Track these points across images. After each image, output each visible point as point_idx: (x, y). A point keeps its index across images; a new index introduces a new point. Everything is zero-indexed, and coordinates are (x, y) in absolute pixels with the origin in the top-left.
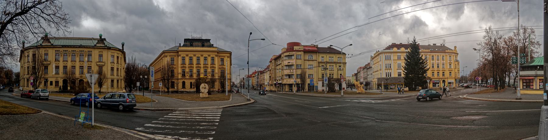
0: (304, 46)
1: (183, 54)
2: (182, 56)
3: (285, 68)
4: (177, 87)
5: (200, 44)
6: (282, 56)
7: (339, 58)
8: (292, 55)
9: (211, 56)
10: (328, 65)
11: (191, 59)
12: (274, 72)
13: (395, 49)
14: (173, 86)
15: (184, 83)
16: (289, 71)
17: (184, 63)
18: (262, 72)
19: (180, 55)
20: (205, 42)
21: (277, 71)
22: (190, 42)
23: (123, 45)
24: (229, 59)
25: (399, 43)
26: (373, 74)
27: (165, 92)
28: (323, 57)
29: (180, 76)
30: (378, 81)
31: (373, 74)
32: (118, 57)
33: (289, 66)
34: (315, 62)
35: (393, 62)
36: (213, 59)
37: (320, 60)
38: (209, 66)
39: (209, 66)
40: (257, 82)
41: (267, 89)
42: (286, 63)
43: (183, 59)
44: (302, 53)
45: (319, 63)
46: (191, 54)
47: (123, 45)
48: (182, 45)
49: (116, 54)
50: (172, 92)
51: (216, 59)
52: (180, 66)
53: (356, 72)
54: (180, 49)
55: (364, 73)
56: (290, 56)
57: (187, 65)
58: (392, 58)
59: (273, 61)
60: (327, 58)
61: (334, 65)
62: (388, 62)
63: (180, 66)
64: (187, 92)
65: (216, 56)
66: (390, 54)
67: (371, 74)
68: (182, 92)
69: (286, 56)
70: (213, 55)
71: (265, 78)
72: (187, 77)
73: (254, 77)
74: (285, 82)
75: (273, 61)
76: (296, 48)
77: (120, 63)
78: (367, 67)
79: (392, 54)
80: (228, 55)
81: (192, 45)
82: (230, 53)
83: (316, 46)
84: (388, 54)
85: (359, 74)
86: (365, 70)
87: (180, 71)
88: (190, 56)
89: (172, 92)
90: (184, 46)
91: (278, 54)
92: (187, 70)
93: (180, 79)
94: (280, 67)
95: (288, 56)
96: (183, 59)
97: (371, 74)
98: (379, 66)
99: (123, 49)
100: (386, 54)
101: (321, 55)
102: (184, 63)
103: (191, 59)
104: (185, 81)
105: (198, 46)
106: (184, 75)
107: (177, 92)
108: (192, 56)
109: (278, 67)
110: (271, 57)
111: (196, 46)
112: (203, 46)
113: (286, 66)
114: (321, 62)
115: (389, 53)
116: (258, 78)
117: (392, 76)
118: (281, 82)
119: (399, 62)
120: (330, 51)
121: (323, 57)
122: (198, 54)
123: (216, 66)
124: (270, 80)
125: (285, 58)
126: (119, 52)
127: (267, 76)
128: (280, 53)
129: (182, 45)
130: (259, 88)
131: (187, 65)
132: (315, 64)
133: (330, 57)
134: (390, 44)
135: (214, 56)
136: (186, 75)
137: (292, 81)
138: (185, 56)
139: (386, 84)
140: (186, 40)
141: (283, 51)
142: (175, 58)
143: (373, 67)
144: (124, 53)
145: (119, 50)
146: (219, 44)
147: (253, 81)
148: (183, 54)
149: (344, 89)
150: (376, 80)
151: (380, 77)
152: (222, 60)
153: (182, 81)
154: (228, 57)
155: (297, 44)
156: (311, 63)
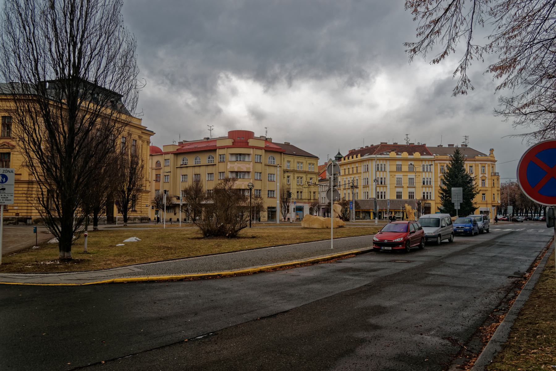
7: (310, 164)
35: (388, 174)
58: (388, 169)
66: (384, 162)
79: (388, 163)
84: (381, 162)
100: (378, 162)
119: (399, 175)
121: (289, 162)
133: (298, 163)
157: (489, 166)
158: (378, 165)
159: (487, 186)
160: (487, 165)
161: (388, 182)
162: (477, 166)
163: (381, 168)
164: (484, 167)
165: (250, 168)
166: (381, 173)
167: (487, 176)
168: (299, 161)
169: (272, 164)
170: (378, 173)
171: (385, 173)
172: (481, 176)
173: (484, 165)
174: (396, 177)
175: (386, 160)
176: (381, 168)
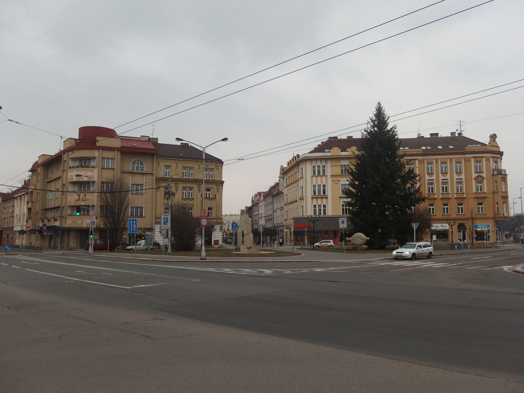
0: (124, 139)
3: (70, 188)
6: (65, 157)
8: (90, 159)
10: (180, 186)
13: (336, 151)
21: (50, 196)
25: (345, 137)
26: (286, 208)
28: (167, 167)
30: (296, 226)
31: (286, 208)
33: (83, 185)
34: (149, 177)
35: (330, 179)
37: (161, 175)
42: (72, 175)
44: (117, 155)
45: (159, 180)
53: (250, 204)
55: (266, 206)
58: (329, 171)
60: (177, 169)
61: (195, 186)
62: (319, 181)
67: (282, 209)
69: (74, 159)
74: (69, 223)
76: (102, 141)
78: (274, 193)
83: (154, 141)
84: (319, 163)
85: (255, 209)
86: (269, 200)
94: (58, 185)
95: (81, 159)
97: (282, 209)
98: (300, 190)
100: (314, 164)
101: (163, 163)
109: (53, 186)
113: (74, 183)
114: (164, 180)
115: (321, 159)
117: (330, 213)
118: (57, 224)
120: (186, 153)
124: (29, 218)
125: (71, 164)
127: (20, 209)
132: (146, 181)
133: (185, 168)
134: (325, 139)
139: (310, 231)
141: (68, 146)
143: (285, 191)
149: (216, 242)
150: (292, 222)
151: (300, 215)
155: (109, 133)
156: (138, 179)
157: (488, 160)
158: (314, 167)
159: (486, 191)
160: (484, 159)
161: (329, 193)
162: (468, 160)
163: (319, 171)
164: (480, 161)
165: (93, 176)
166: (319, 178)
167: (484, 175)
168: (185, 165)
169: (140, 171)
170: (314, 178)
171: (324, 178)
172: (474, 175)
173: (478, 159)
174: (342, 183)
175: (326, 159)
176: (319, 171)
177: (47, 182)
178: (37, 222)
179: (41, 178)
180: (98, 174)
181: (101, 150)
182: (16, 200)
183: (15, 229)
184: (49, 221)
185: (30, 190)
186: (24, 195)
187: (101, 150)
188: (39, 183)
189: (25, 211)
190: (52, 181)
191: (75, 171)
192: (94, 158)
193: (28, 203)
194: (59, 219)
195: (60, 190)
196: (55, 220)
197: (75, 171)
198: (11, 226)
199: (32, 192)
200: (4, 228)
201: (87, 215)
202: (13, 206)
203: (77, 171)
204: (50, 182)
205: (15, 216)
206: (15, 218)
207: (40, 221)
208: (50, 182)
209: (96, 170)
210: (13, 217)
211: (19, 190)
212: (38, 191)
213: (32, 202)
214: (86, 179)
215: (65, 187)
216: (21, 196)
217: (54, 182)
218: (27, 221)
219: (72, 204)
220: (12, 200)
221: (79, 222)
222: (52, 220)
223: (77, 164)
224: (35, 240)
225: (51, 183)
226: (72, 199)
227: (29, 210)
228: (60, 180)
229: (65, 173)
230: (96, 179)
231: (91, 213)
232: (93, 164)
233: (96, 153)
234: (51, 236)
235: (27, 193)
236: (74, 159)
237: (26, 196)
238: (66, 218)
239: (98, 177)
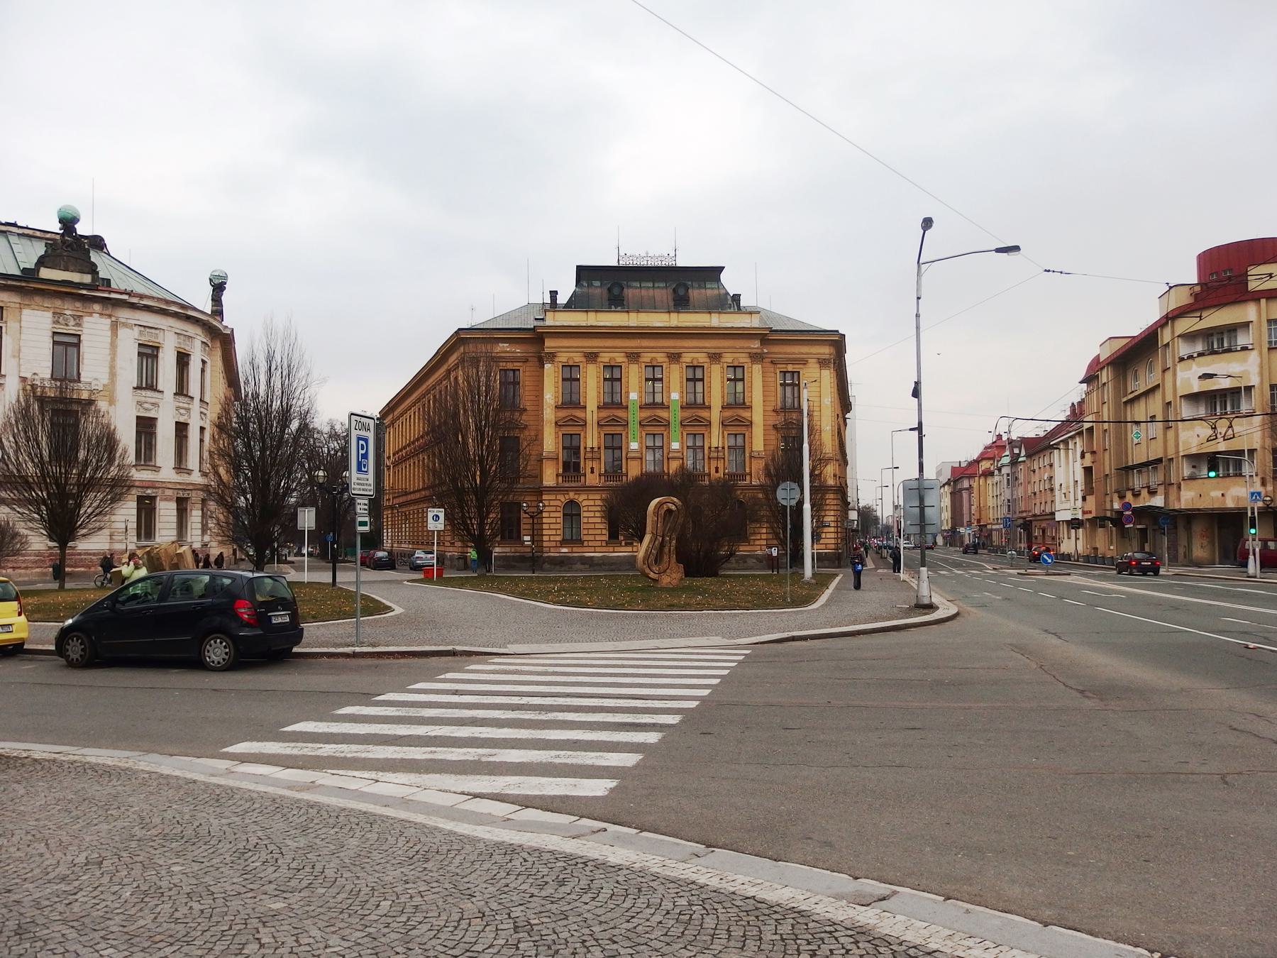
1: (568, 351)
2: (563, 358)
3: (1186, 411)
4: (537, 534)
5: (662, 293)
6: (1166, 336)
8: (1232, 329)
9: (728, 358)
11: (613, 377)
12: (1110, 442)
14: (510, 531)
15: (572, 513)
16: (1204, 430)
17: (571, 402)
18: (1037, 447)
19: (552, 357)
20: (688, 284)
21: (1134, 434)
22: (605, 284)
23: (218, 288)
24: (828, 376)
27: (464, 563)
29: (550, 476)
32: (183, 360)
33: (1219, 401)
36: (737, 375)
38: (715, 415)
39: (715, 415)
40: (1011, 504)
41: (1067, 546)
43: (571, 378)
46: (613, 353)
47: (218, 288)
48: (562, 299)
49: (169, 339)
50: (508, 563)
51: (756, 373)
52: (549, 414)
54: (553, 320)
56: (1219, 341)
57: (591, 411)
59: (1105, 376)
63: (549, 414)
64: (590, 563)
65: (756, 357)
68: (562, 562)
69: (1190, 337)
70: (735, 353)
71: (1060, 476)
72: (592, 480)
73: (988, 474)
74: (1187, 498)
75: (1105, 376)
77: (194, 388)
80: (826, 351)
81: (616, 302)
82: (837, 343)
87: (550, 442)
88: (605, 358)
89: (508, 563)
90: (572, 305)
91: (1135, 327)
92: (592, 439)
93: (551, 490)
94: (1154, 406)
96: (571, 378)
99: (218, 312)
102: (571, 402)
103: (613, 377)
104: (581, 498)
105: (653, 307)
106: (571, 468)
107: (534, 561)
108: (620, 358)
109: (1140, 412)
110: (1091, 345)
111: (640, 307)
112: (681, 303)
113: (1194, 398)
116: (1013, 480)
118: (1158, 501)
122: (654, 352)
123: (758, 416)
124: (1089, 490)
125: (1184, 349)
126: (192, 330)
127: (1067, 469)
128: (1152, 315)
129: (562, 299)
130: (1029, 537)
131: (591, 411)
135: (743, 359)
136: (586, 466)
137: (1235, 494)
138: (578, 358)
140: (584, 273)
142: (526, 376)
144: (224, 341)
145: (184, 314)
146: (768, 286)
147: (992, 499)
148: (568, 351)
152: (792, 382)
153: (563, 498)
154: (823, 363)
177: (1126, 403)
178: (1108, 499)
179: (1109, 393)
180: (1261, 367)
181: (1263, 301)
182: (1056, 452)
183: (1058, 517)
184: (1136, 495)
185: (1087, 426)
186: (1072, 437)
187: (1263, 301)
188: (1106, 406)
189: (1080, 475)
190: (1137, 398)
191: (1194, 367)
192: (1246, 325)
193: (1083, 456)
194: (1161, 489)
195: (1160, 417)
196: (1152, 493)
197: (1194, 367)
198: (1048, 510)
199: (1090, 430)
200: (1035, 515)
201: (1236, 475)
202: (1051, 465)
203: (1199, 365)
204: (1132, 401)
205: (1057, 487)
206: (1057, 493)
207: (1116, 496)
208: (1132, 401)
209: (1253, 357)
210: (1052, 490)
211: (1065, 424)
212: (1106, 426)
213: (1093, 453)
214: (1225, 384)
215: (1172, 409)
216: (1066, 442)
217: (1142, 401)
218: (1084, 499)
219: (1194, 451)
220: (1047, 453)
221: (1216, 494)
222: (1144, 492)
223: (1199, 347)
224: (1105, 543)
225: (1136, 405)
226: (1194, 437)
227: (1088, 471)
228: (1158, 395)
229: (1169, 375)
230: (1254, 380)
231: (1246, 469)
232: (1242, 340)
233: (1249, 312)
234: (1143, 531)
235: (1080, 434)
236: (1190, 337)
237: (1078, 440)
238: (1179, 488)
239: (1261, 374)
